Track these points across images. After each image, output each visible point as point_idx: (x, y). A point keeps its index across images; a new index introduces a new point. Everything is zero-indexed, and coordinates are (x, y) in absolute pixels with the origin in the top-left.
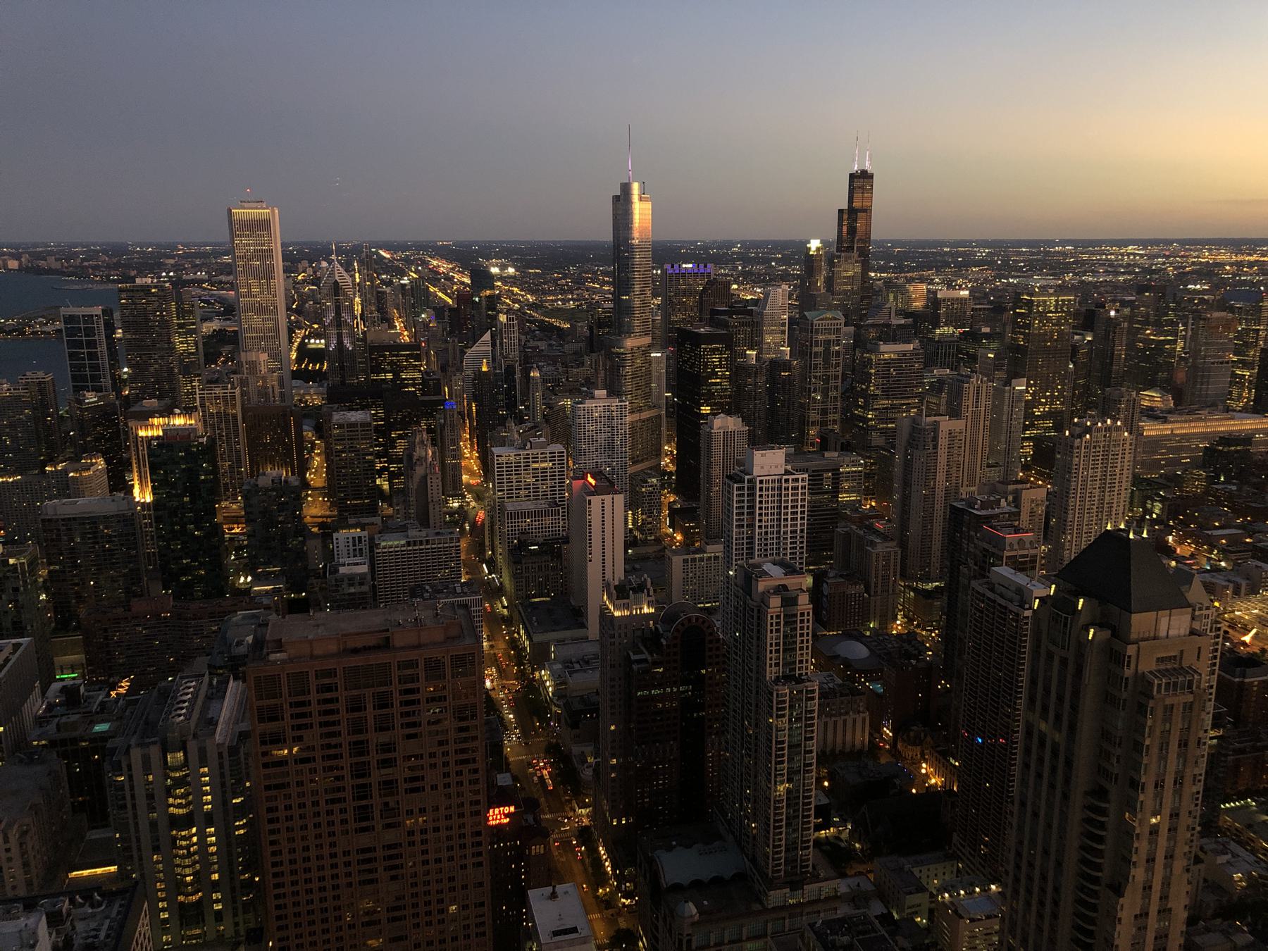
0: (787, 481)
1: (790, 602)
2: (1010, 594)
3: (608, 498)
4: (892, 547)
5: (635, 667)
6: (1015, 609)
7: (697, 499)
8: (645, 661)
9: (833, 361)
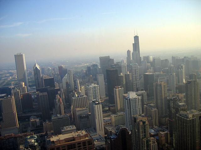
0: (137, 98)
1: (144, 123)
2: (184, 116)
3: (98, 105)
4: (156, 109)
5: (112, 140)
6: (186, 119)
7: (115, 104)
8: (114, 138)
9: (137, 73)
